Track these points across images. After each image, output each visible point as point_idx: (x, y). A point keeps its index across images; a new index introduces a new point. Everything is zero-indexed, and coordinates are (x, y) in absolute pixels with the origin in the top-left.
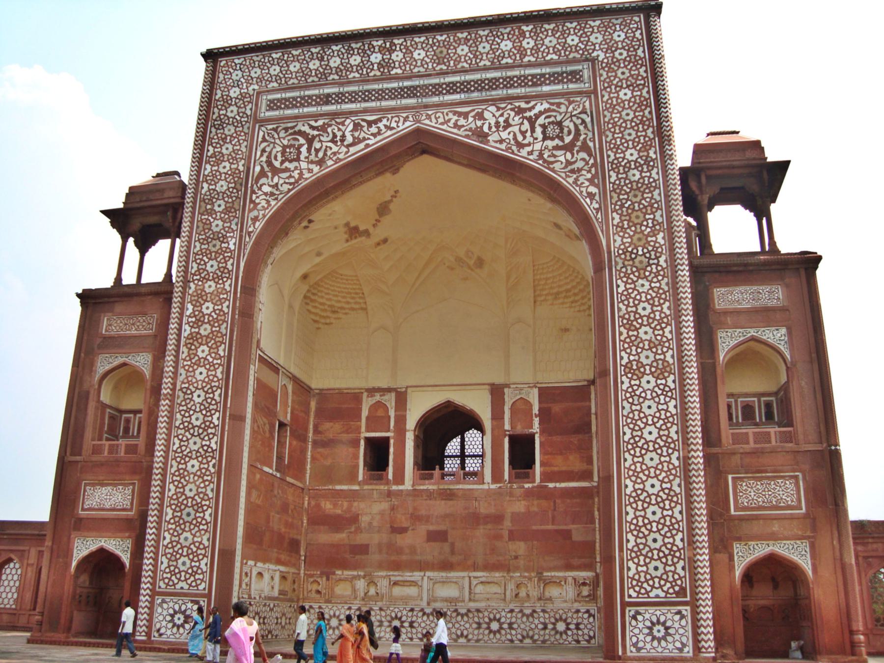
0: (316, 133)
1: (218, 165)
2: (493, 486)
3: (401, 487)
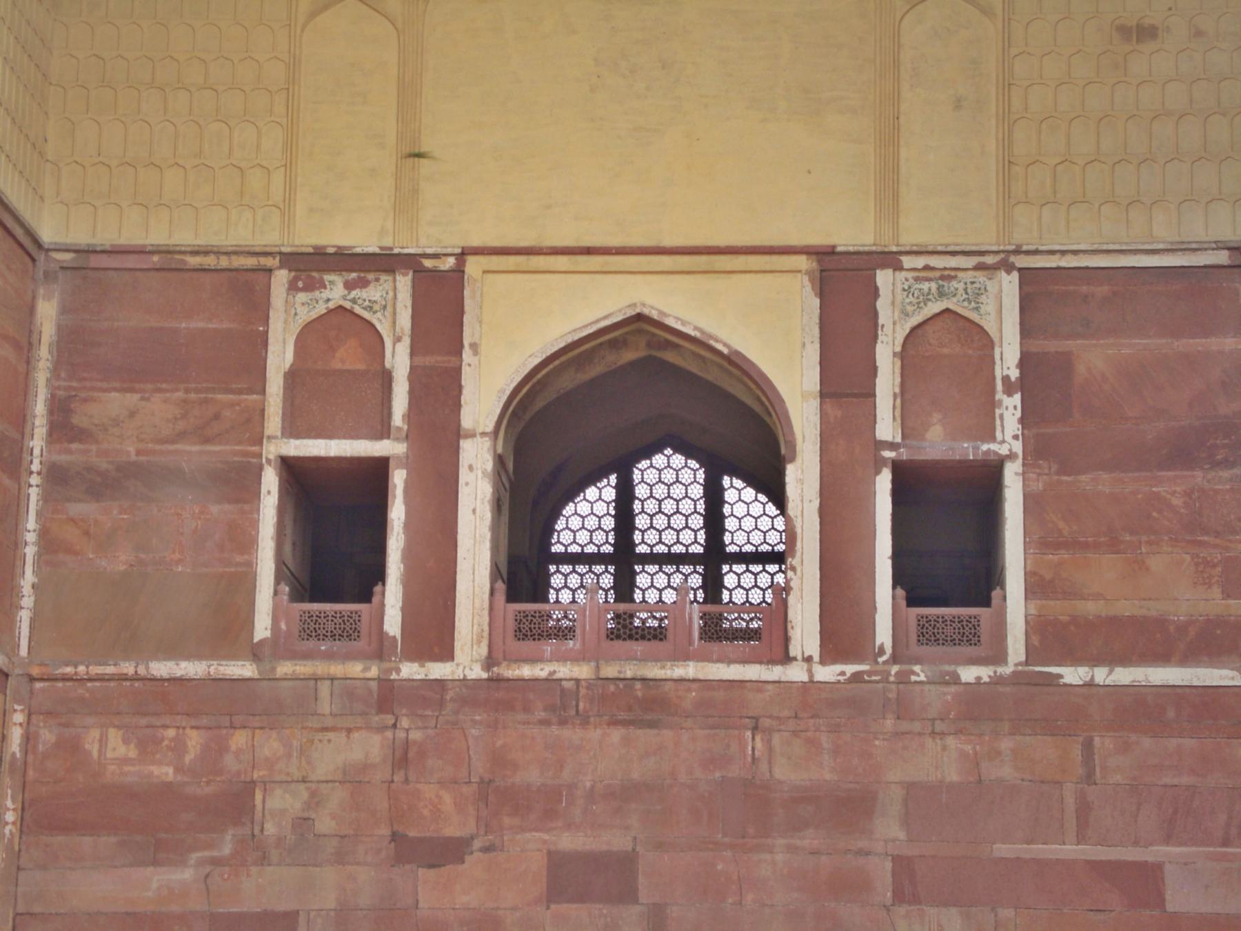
2: (826, 673)
3: (438, 670)
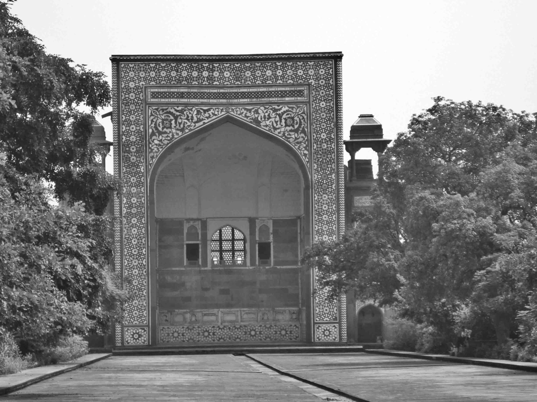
0: (178, 114)
1: (129, 127)
2: (251, 268)
3: (206, 269)
